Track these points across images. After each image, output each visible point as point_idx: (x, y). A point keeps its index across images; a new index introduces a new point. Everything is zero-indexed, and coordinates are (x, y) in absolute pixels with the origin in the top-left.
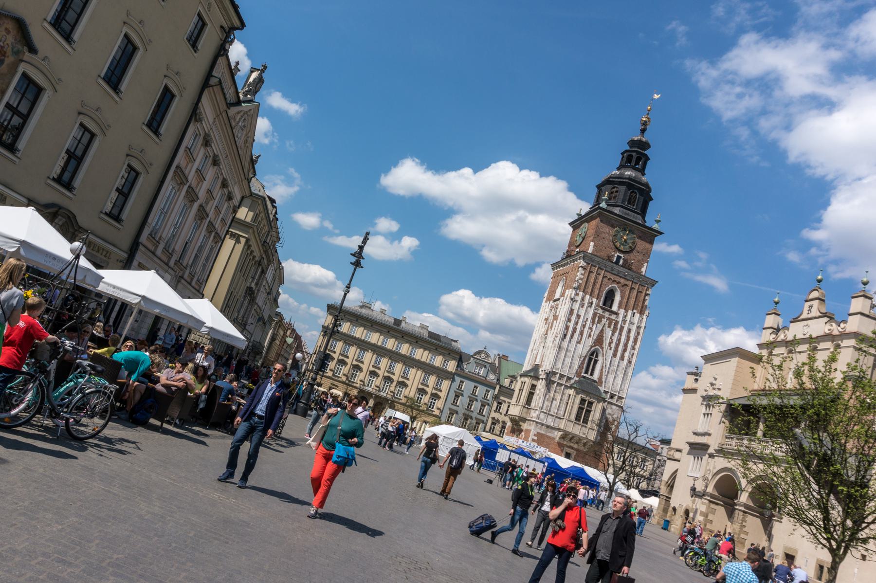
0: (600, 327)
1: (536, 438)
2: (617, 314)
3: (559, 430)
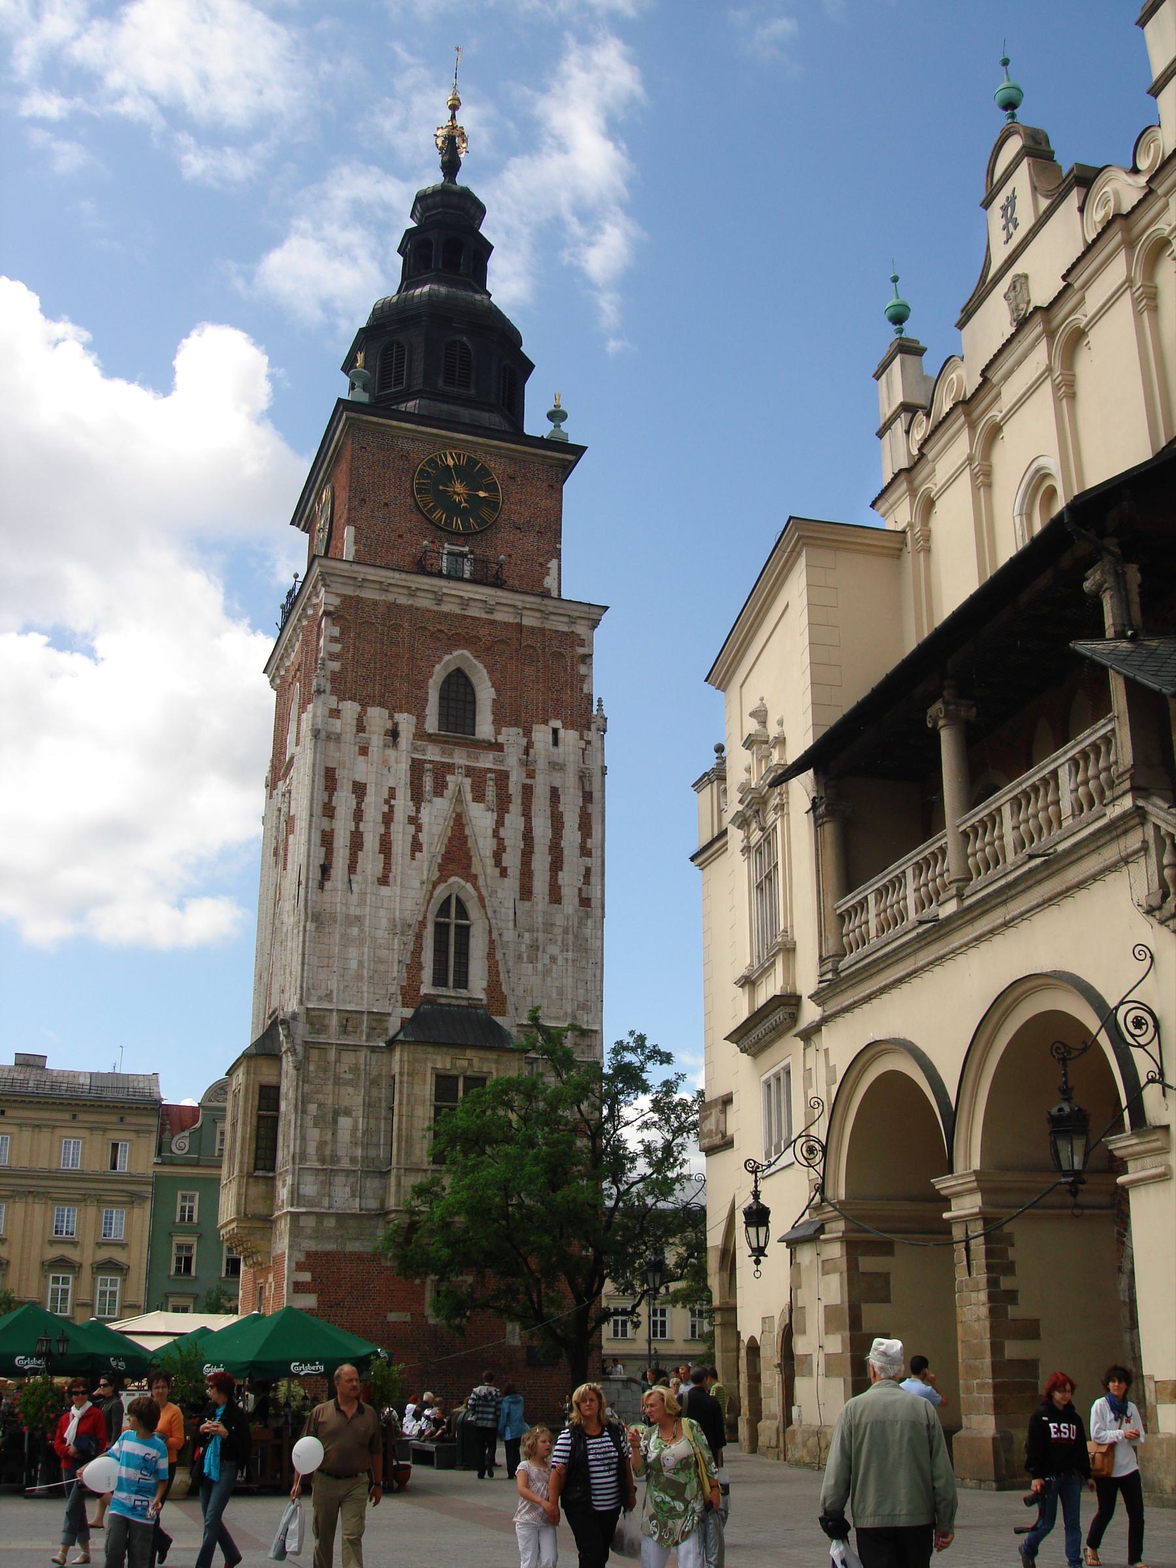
1: (306, 1277)
2: (498, 747)
3: (383, 1213)
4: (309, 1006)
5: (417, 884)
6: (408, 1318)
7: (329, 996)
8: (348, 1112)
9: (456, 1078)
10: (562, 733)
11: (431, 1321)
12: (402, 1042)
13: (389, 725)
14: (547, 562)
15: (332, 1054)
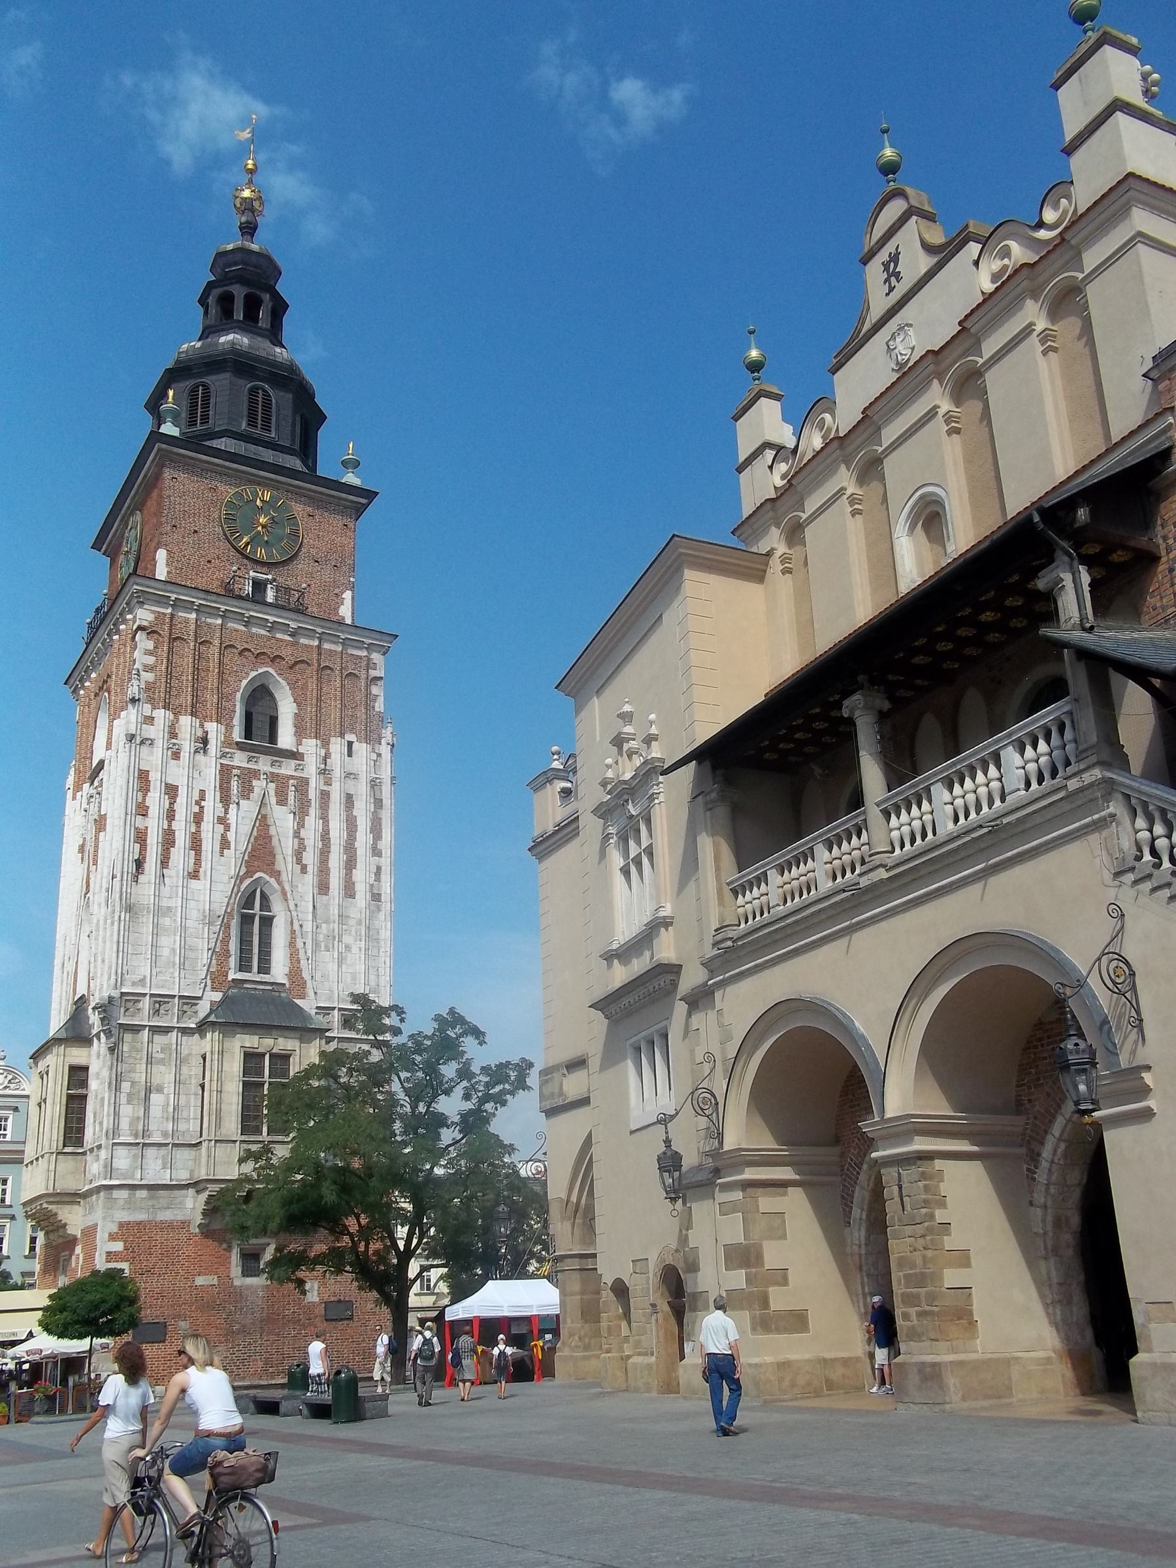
0: (249, 808)
1: (119, 1246)
5: (225, 879)
6: (215, 1282)
7: (142, 981)
8: (160, 1090)
9: (263, 1055)
10: (356, 746)
11: (237, 1283)
12: (213, 1023)
13: (200, 733)
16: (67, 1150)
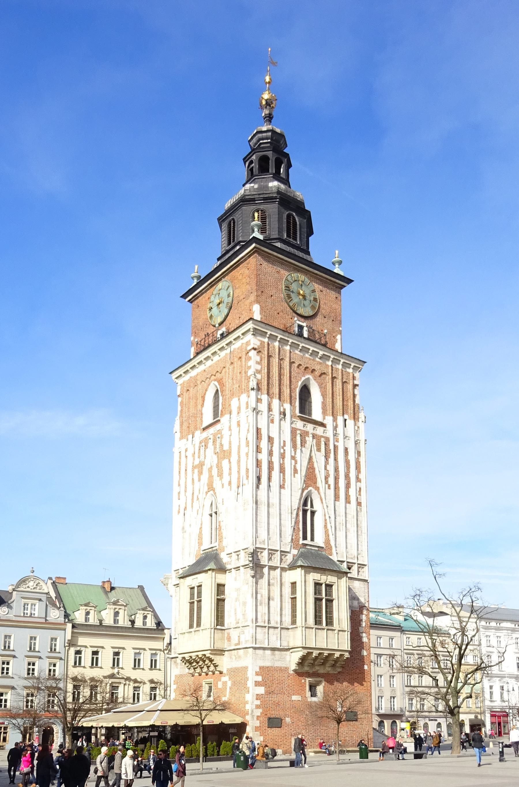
1: (259, 679)
4: (257, 546)
6: (300, 699)
9: (321, 584)
12: (301, 566)
14: (336, 336)
15: (266, 570)
16: (218, 627)
